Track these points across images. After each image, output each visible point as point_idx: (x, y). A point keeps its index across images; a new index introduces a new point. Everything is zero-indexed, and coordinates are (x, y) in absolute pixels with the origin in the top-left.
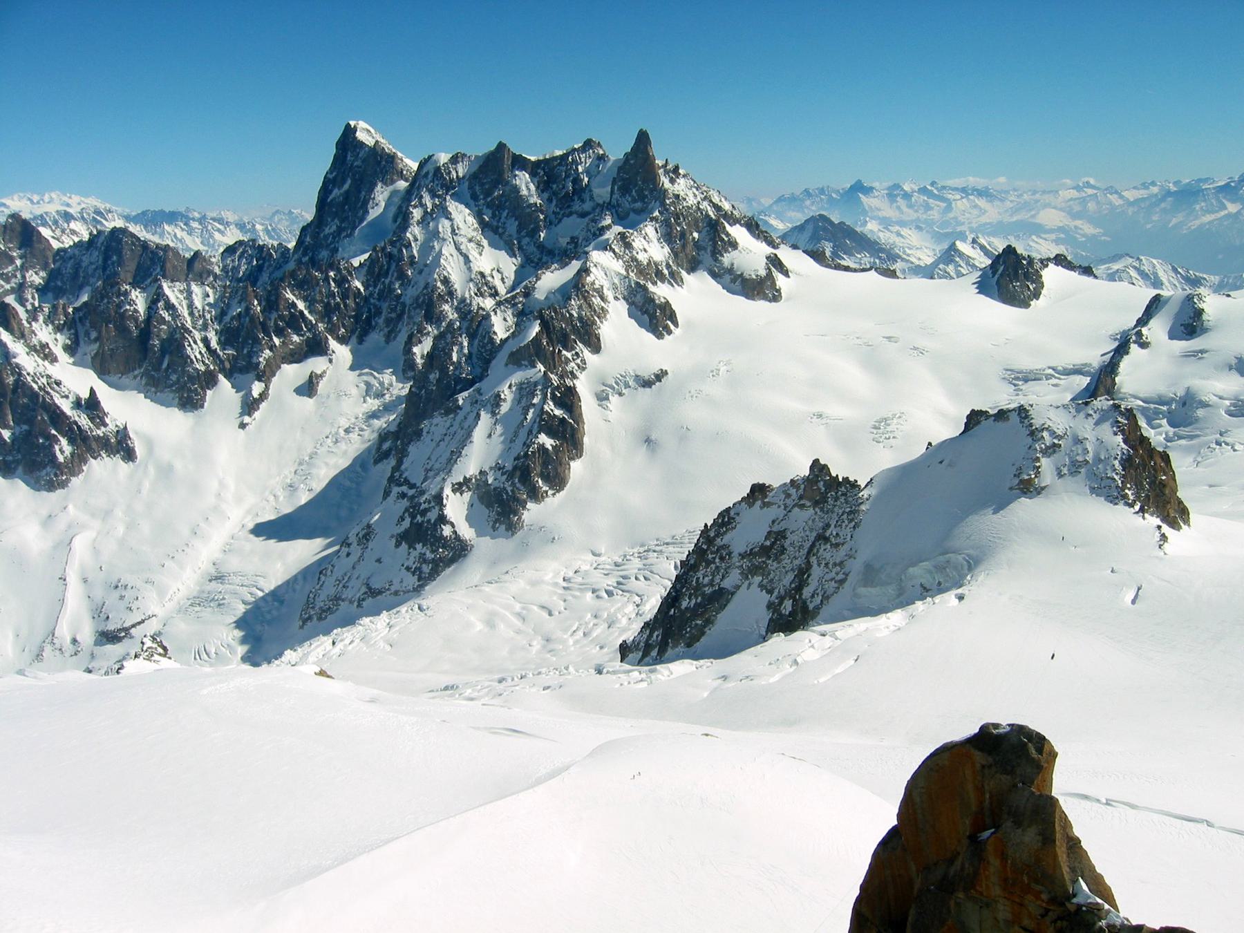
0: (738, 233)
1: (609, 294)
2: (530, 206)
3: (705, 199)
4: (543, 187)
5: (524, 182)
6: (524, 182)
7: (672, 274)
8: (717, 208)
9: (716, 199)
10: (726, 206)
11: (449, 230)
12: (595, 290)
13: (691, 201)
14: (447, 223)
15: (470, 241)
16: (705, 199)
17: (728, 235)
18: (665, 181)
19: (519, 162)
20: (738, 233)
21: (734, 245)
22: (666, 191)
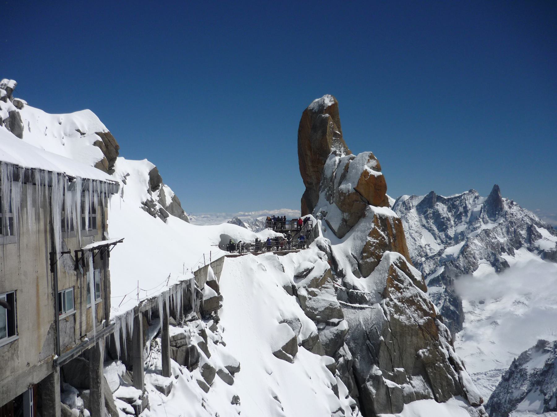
0: (543, 232)
1: (477, 256)
2: (443, 218)
3: (526, 215)
4: (450, 210)
5: (442, 208)
6: (442, 208)
7: (509, 249)
8: (531, 219)
9: (531, 216)
10: (537, 219)
11: (408, 227)
12: (471, 254)
13: (519, 216)
14: (406, 224)
15: (416, 232)
16: (526, 215)
17: (537, 232)
18: (506, 208)
19: (440, 199)
20: (543, 232)
21: (540, 236)
22: (507, 212)
